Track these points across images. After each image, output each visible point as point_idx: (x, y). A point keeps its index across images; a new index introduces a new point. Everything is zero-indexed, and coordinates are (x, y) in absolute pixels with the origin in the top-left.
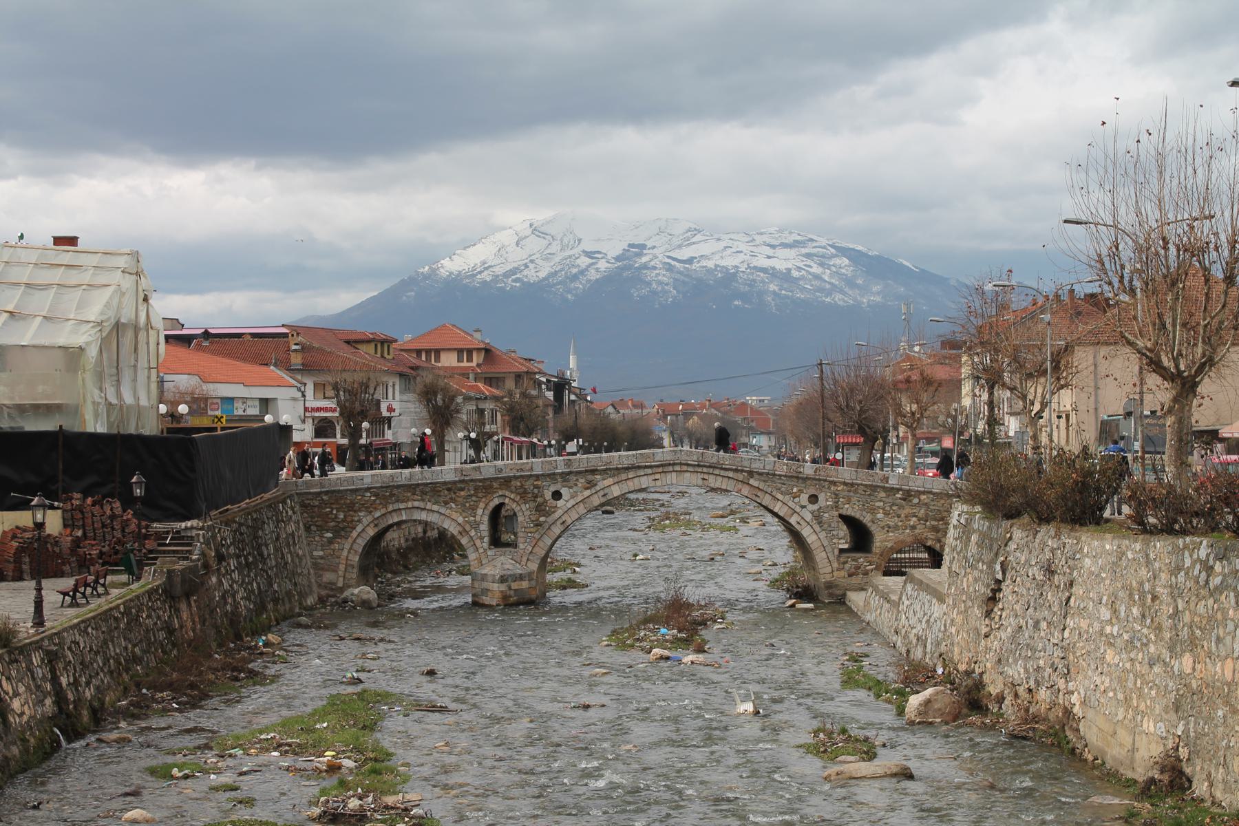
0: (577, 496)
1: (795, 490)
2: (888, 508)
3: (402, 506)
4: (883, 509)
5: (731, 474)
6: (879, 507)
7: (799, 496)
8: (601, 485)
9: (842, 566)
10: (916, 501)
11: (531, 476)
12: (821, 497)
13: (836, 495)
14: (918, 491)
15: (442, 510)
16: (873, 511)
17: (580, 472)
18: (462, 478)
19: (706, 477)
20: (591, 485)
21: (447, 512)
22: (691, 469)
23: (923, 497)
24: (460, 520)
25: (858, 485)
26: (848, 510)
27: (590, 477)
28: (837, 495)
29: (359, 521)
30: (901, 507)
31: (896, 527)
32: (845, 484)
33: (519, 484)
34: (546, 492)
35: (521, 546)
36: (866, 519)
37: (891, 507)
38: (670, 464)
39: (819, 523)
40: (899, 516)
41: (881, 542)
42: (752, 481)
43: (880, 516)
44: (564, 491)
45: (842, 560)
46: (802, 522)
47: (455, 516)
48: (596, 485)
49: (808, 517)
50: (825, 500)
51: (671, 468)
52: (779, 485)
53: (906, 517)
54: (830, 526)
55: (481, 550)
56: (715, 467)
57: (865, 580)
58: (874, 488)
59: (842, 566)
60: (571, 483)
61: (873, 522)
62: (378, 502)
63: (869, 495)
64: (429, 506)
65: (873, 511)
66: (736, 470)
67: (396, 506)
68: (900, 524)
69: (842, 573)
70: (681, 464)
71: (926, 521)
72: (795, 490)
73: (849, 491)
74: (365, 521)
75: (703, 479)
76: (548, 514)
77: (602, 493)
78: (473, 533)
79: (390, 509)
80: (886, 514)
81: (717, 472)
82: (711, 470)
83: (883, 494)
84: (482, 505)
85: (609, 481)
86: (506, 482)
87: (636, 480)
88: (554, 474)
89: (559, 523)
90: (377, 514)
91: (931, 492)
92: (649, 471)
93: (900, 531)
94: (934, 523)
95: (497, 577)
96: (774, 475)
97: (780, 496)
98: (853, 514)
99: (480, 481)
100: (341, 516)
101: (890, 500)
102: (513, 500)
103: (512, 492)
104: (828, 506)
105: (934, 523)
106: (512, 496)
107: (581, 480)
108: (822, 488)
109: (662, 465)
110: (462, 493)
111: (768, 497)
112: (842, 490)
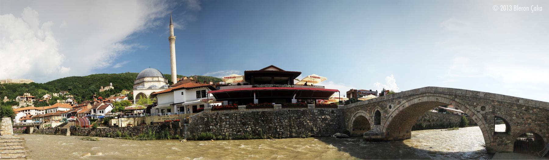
1: (475, 104)
2: (518, 114)
4: (516, 115)
5: (447, 96)
6: (514, 114)
7: (477, 107)
9: (495, 140)
10: (531, 112)
12: (487, 107)
13: (494, 107)
14: (532, 107)
19: (438, 98)
22: (432, 95)
23: (535, 110)
25: (505, 102)
28: (494, 107)
30: (524, 114)
31: (521, 124)
32: (498, 102)
37: (519, 114)
38: (424, 93)
39: (486, 119)
40: (523, 118)
41: (514, 130)
42: (456, 100)
43: (514, 118)
45: (495, 137)
46: (478, 119)
49: (481, 117)
52: (468, 102)
53: (526, 119)
54: (490, 121)
56: (441, 93)
57: (505, 148)
59: (495, 140)
61: (511, 120)
63: (510, 108)
65: (511, 115)
66: (450, 95)
68: (523, 122)
69: (495, 144)
70: (428, 93)
71: (536, 121)
72: (475, 104)
73: (500, 105)
75: (437, 99)
80: (517, 117)
81: (442, 95)
82: (440, 95)
83: (516, 108)
91: (538, 108)
93: (523, 125)
94: (539, 122)
96: (466, 97)
97: (468, 106)
101: (519, 110)
104: (490, 112)
105: (539, 122)
108: (487, 103)
112: (497, 105)
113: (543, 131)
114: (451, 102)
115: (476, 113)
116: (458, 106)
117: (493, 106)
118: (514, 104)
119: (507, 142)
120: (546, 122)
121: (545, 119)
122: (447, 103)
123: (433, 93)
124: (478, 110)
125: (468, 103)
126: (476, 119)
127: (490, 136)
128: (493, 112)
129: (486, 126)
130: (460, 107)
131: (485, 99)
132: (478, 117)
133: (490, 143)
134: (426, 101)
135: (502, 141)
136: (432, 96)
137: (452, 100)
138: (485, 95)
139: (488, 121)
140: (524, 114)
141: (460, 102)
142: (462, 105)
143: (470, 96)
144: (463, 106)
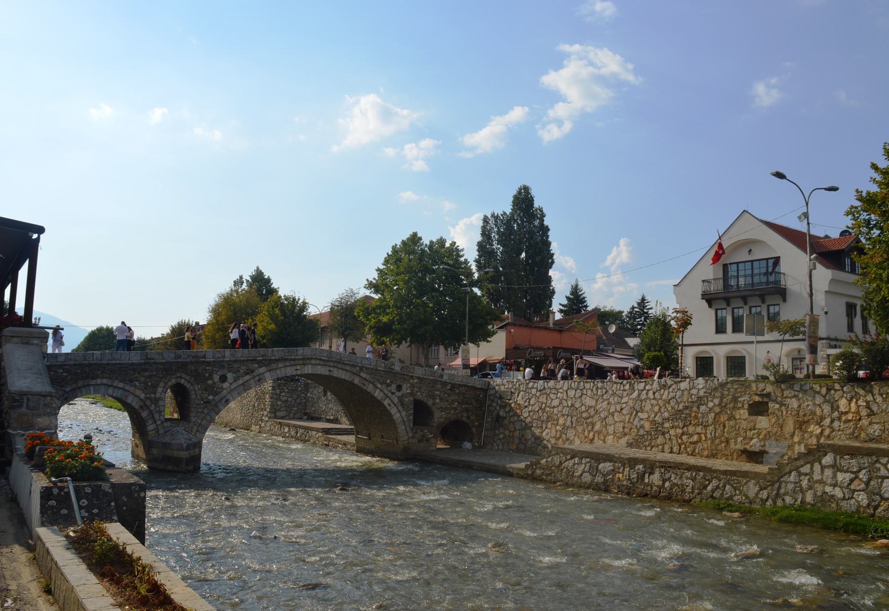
0: (239, 379)
1: (388, 381)
3: (93, 382)
4: (439, 396)
5: (348, 368)
8: (257, 372)
10: (457, 391)
11: (204, 362)
12: (404, 387)
13: (412, 386)
15: (127, 388)
16: (433, 397)
17: (243, 361)
18: (147, 361)
19: (332, 369)
21: (132, 389)
24: (143, 396)
26: (419, 396)
30: (449, 395)
32: (418, 378)
33: (193, 368)
34: (215, 375)
35: (193, 419)
36: (430, 402)
37: (443, 394)
39: (402, 405)
40: (448, 401)
41: (437, 419)
42: (362, 374)
43: (437, 401)
44: (230, 376)
46: (391, 404)
47: (138, 392)
48: (253, 371)
49: (396, 400)
50: (406, 389)
51: (308, 362)
53: (452, 402)
54: (408, 407)
55: (159, 422)
58: (435, 382)
62: (69, 378)
64: (116, 383)
65: (433, 397)
68: (448, 406)
69: (415, 441)
70: (316, 359)
72: (388, 381)
75: (330, 371)
76: (216, 394)
77: (257, 378)
79: (79, 385)
80: (441, 399)
81: (340, 366)
82: (336, 365)
83: (439, 386)
84: (162, 384)
87: (283, 370)
88: (223, 361)
89: (223, 401)
90: (68, 389)
91: (466, 386)
93: (448, 411)
94: (467, 406)
95: (185, 446)
96: (377, 370)
98: (422, 399)
99: (162, 364)
102: (189, 382)
103: (187, 374)
104: (408, 393)
105: (467, 406)
106: (187, 378)
107: (242, 367)
108: (405, 380)
109: (303, 359)
110: (146, 374)
111: (371, 386)
112: (417, 383)
113: (472, 417)
114: (353, 377)
115: (390, 395)
116: (364, 384)
117: (411, 384)
118: (438, 381)
119: (429, 436)
120: (475, 405)
121: (473, 400)
122: (346, 379)
123: (324, 360)
124: (393, 391)
125: (378, 380)
126: (389, 405)
127: (409, 430)
128: (411, 394)
129: (403, 415)
130: (367, 385)
131: (401, 374)
132: (392, 401)
133: (408, 438)
134: (310, 372)
135: (423, 436)
136: (321, 365)
137: (354, 373)
138: (401, 369)
139: (406, 407)
140: (449, 395)
141: (367, 378)
142: (370, 382)
143: (383, 369)
144: (371, 384)
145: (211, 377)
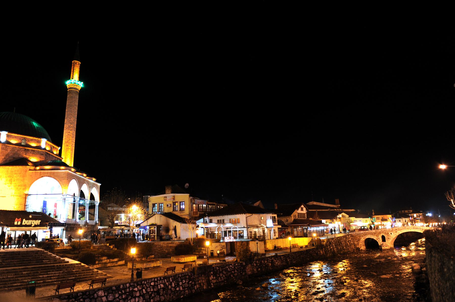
3: (367, 236)
20: (396, 232)
21: (374, 237)
24: (376, 238)
27: (396, 231)
29: (361, 238)
44: (392, 233)
60: (393, 232)
66: (420, 229)
67: (367, 236)
74: (362, 238)
76: (390, 237)
78: (378, 240)
81: (417, 229)
85: (399, 231)
86: (383, 232)
92: (405, 230)
100: (359, 237)
145: (388, 234)
